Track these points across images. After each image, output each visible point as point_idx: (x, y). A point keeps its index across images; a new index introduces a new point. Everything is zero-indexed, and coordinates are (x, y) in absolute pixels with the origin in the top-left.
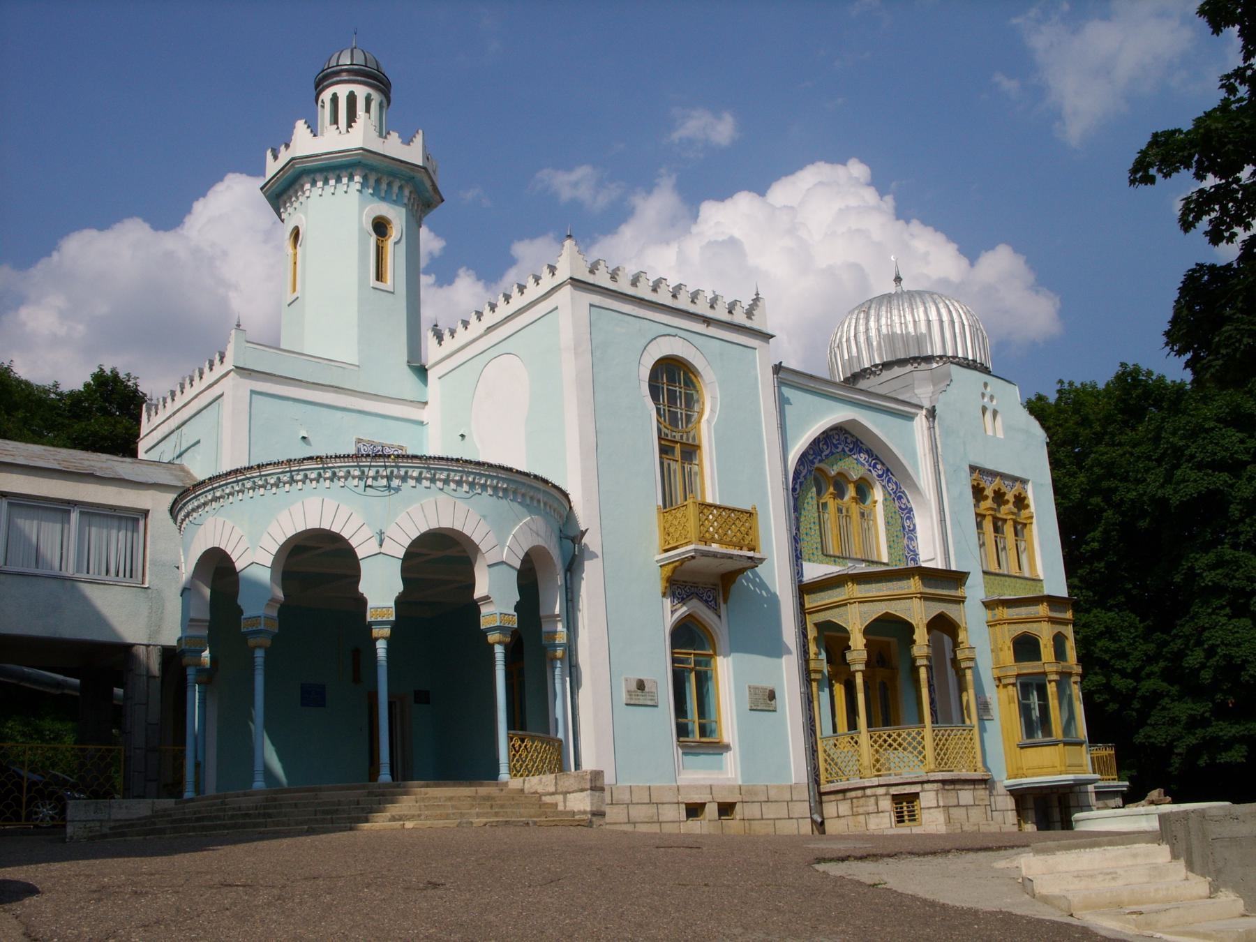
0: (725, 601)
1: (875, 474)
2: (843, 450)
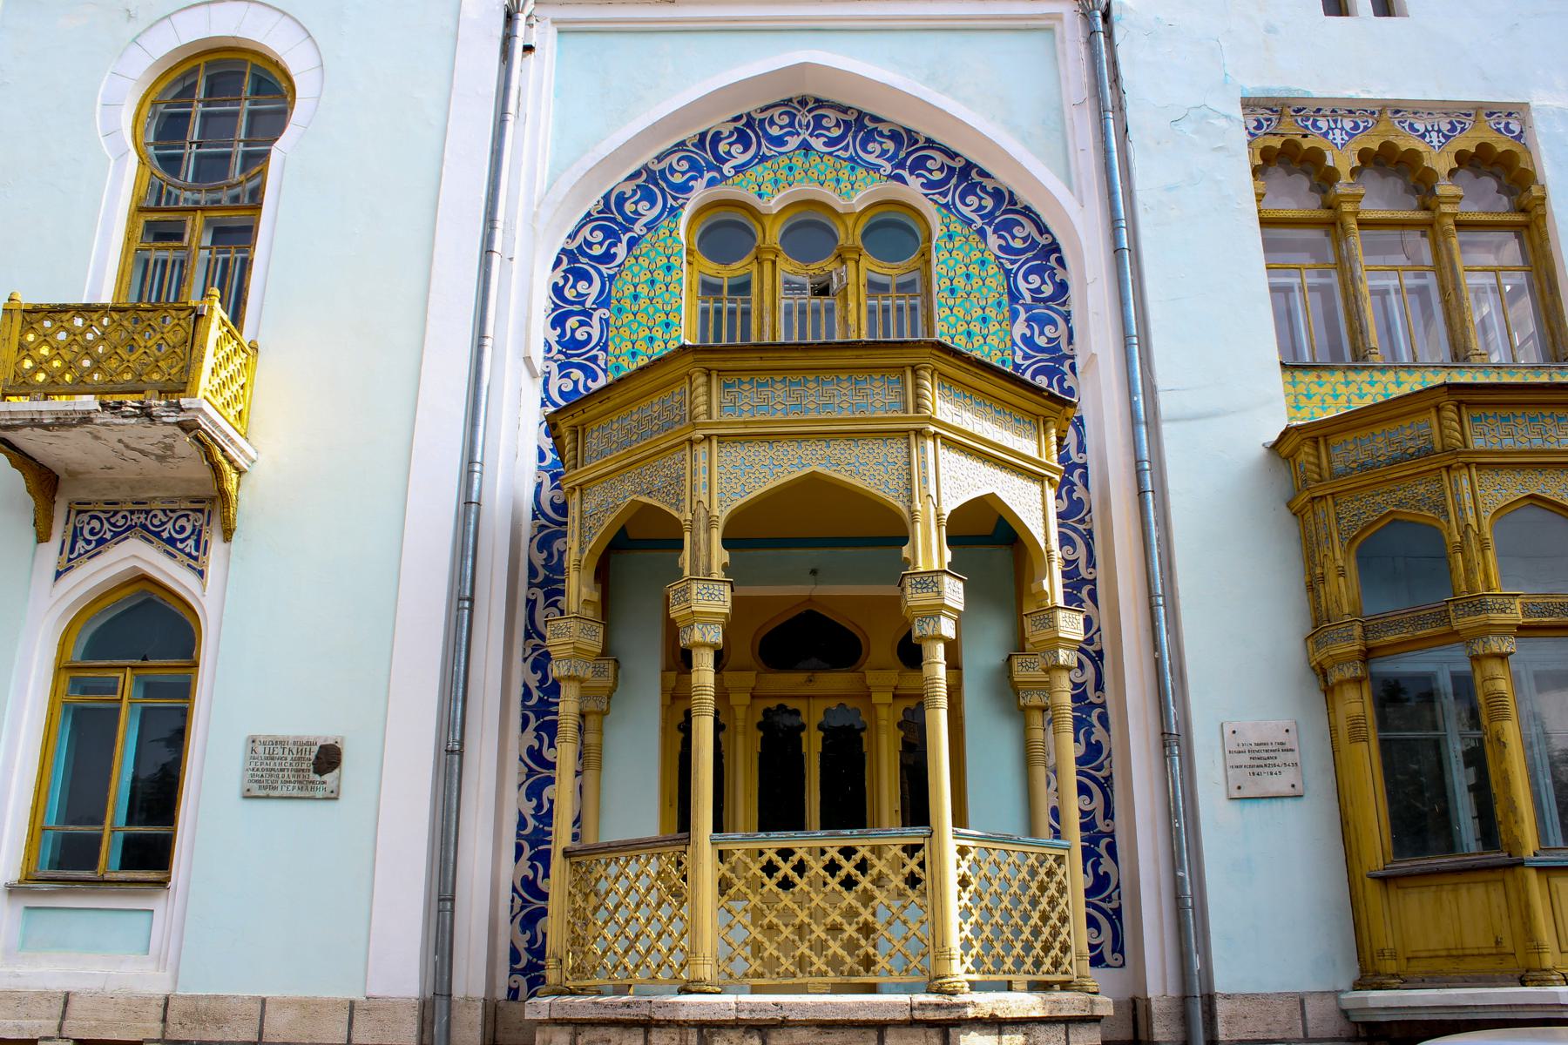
0: (228, 534)
1: (915, 183)
2: (806, 147)
